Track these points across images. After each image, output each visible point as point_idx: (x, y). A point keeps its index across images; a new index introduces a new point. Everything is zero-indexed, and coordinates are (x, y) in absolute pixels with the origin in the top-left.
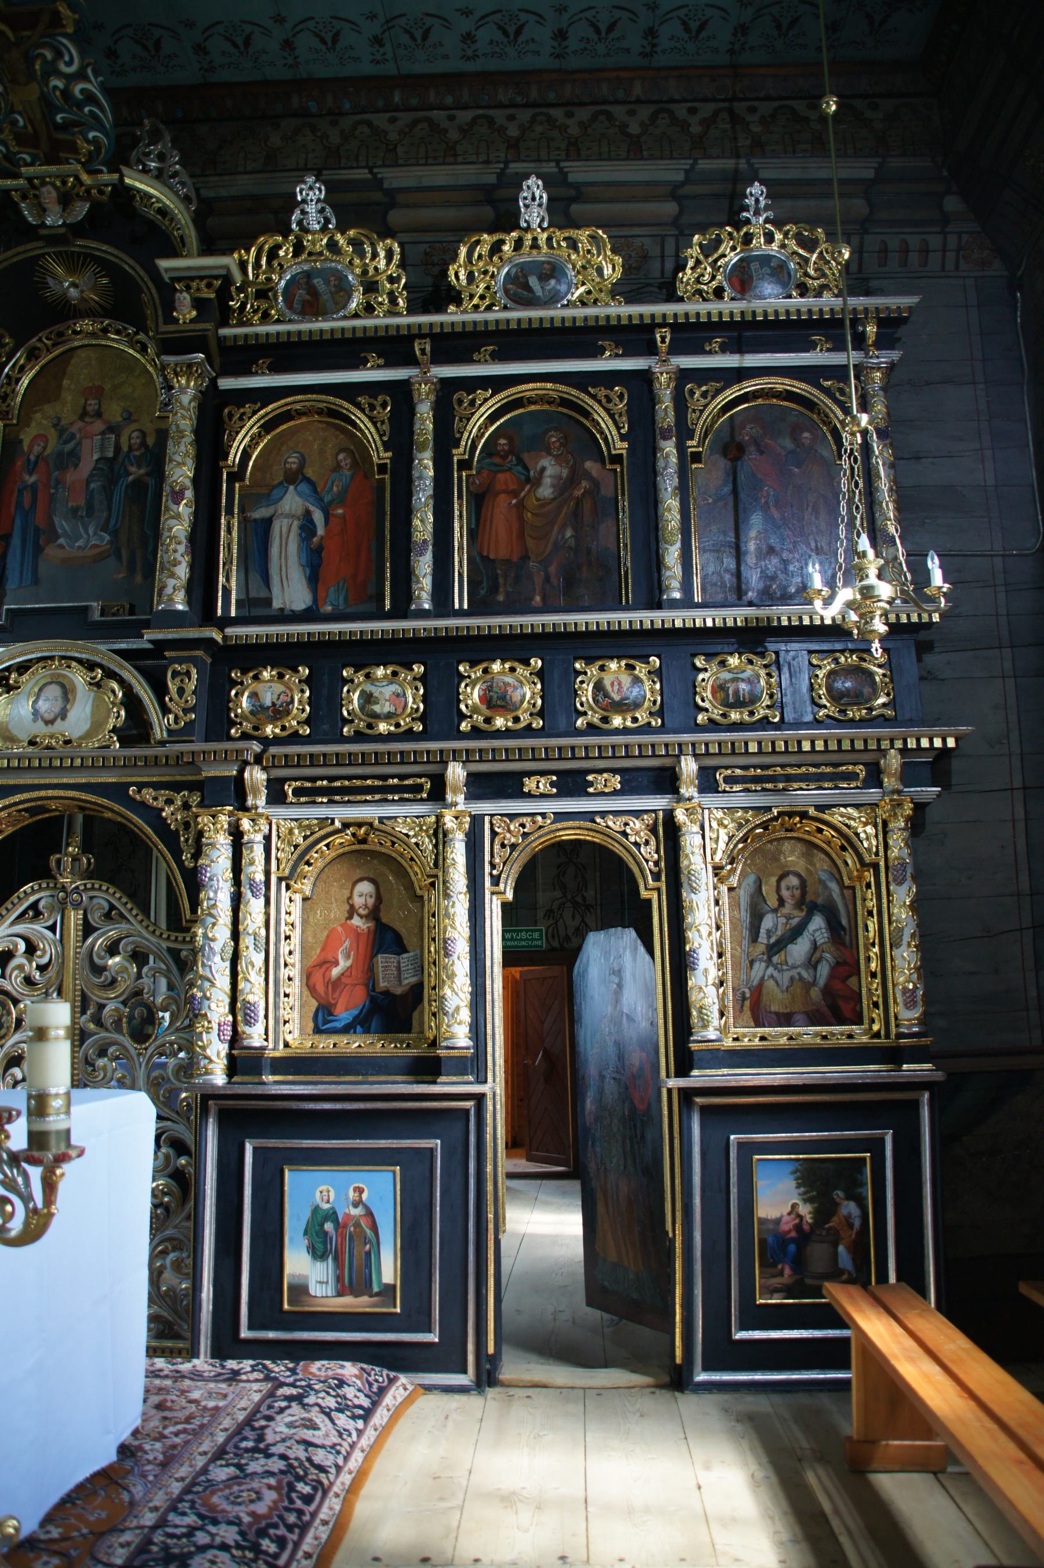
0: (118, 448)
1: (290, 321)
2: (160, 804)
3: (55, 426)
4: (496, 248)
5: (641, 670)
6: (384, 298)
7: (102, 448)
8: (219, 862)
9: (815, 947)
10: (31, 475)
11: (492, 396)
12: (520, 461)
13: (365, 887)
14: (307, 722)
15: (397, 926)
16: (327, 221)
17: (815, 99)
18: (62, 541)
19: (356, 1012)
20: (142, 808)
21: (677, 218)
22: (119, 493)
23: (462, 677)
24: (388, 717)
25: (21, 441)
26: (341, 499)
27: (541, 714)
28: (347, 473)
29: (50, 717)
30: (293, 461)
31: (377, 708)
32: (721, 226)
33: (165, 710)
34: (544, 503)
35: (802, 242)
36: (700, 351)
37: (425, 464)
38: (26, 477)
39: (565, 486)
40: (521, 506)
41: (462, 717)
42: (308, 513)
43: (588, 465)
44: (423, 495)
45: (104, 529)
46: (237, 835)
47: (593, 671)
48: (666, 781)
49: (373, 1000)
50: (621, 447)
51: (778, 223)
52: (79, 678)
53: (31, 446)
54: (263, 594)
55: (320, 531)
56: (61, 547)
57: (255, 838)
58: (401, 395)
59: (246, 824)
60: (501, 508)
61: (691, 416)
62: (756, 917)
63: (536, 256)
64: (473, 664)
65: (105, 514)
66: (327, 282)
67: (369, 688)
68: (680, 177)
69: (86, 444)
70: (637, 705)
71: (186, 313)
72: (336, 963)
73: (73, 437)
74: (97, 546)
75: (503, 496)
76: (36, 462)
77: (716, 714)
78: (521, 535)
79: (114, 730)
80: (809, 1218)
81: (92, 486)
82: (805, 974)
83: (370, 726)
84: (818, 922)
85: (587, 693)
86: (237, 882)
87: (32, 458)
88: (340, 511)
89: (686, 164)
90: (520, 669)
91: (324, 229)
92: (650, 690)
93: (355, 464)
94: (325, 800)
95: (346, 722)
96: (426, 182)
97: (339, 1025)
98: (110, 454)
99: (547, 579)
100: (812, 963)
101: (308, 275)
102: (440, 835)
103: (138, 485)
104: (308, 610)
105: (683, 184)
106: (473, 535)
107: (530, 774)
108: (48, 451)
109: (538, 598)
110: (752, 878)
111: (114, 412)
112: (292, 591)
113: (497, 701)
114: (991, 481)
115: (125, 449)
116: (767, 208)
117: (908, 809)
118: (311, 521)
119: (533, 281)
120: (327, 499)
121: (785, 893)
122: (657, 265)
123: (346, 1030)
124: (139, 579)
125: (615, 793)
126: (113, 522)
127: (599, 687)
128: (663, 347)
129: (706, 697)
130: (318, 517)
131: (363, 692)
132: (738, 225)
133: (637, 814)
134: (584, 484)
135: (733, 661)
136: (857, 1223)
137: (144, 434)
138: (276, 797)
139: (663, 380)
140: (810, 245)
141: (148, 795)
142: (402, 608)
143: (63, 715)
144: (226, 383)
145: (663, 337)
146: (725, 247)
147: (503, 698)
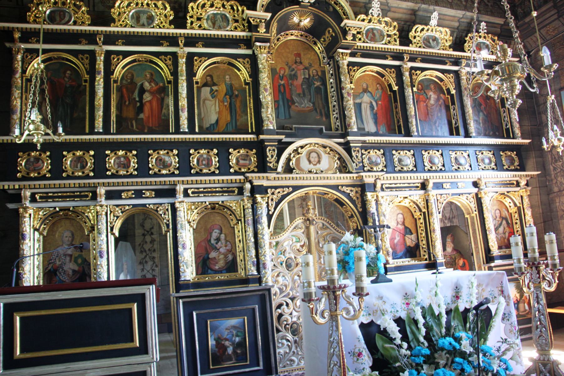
0: (309, 75)
1: (367, 42)
2: (348, 192)
3: (287, 65)
4: (423, 30)
7: (304, 74)
9: (504, 229)
10: (282, 81)
11: (422, 72)
12: (425, 92)
13: (400, 216)
15: (409, 227)
16: (379, 14)
17: (530, 13)
18: (296, 104)
19: (402, 253)
20: (343, 193)
21: (458, 27)
22: (312, 91)
25: (276, 69)
28: (380, 91)
29: (315, 163)
31: (403, 163)
33: (354, 162)
37: (409, 92)
38: (280, 81)
40: (427, 106)
41: (424, 166)
42: (371, 102)
43: (441, 95)
45: (310, 101)
46: (377, 201)
49: (406, 248)
50: (453, 92)
51: (487, 33)
52: (321, 150)
53: (280, 71)
54: (362, 127)
55: (376, 108)
56: (297, 106)
57: (381, 201)
58: (398, 70)
59: (380, 198)
65: (309, 97)
66: (378, 32)
67: (400, 157)
68: (461, 16)
69: (298, 72)
71: (349, 38)
72: (395, 239)
73: (293, 70)
74: (308, 107)
75: (422, 102)
76: (283, 77)
80: (519, 298)
81: (304, 87)
82: (504, 236)
83: (402, 168)
84: (504, 222)
87: (281, 75)
88: (380, 103)
89: (464, 12)
90: (438, 154)
91: (378, 16)
93: (382, 88)
94: (394, 190)
96: (400, 6)
97: (398, 257)
98: (307, 77)
100: (504, 233)
101: (372, 29)
103: (318, 89)
104: (375, 132)
105: (462, 18)
107: (445, 183)
108: (286, 74)
111: (306, 63)
112: (371, 127)
113: (431, 161)
115: (312, 75)
116: (485, 29)
118: (372, 105)
119: (431, 41)
120: (376, 98)
123: (401, 258)
124: (324, 119)
126: (312, 100)
127: (456, 159)
130: (374, 104)
131: (399, 158)
136: (528, 297)
137: (317, 72)
138: (382, 189)
141: (344, 189)
142: (408, 134)
143: (319, 162)
145: (464, 62)
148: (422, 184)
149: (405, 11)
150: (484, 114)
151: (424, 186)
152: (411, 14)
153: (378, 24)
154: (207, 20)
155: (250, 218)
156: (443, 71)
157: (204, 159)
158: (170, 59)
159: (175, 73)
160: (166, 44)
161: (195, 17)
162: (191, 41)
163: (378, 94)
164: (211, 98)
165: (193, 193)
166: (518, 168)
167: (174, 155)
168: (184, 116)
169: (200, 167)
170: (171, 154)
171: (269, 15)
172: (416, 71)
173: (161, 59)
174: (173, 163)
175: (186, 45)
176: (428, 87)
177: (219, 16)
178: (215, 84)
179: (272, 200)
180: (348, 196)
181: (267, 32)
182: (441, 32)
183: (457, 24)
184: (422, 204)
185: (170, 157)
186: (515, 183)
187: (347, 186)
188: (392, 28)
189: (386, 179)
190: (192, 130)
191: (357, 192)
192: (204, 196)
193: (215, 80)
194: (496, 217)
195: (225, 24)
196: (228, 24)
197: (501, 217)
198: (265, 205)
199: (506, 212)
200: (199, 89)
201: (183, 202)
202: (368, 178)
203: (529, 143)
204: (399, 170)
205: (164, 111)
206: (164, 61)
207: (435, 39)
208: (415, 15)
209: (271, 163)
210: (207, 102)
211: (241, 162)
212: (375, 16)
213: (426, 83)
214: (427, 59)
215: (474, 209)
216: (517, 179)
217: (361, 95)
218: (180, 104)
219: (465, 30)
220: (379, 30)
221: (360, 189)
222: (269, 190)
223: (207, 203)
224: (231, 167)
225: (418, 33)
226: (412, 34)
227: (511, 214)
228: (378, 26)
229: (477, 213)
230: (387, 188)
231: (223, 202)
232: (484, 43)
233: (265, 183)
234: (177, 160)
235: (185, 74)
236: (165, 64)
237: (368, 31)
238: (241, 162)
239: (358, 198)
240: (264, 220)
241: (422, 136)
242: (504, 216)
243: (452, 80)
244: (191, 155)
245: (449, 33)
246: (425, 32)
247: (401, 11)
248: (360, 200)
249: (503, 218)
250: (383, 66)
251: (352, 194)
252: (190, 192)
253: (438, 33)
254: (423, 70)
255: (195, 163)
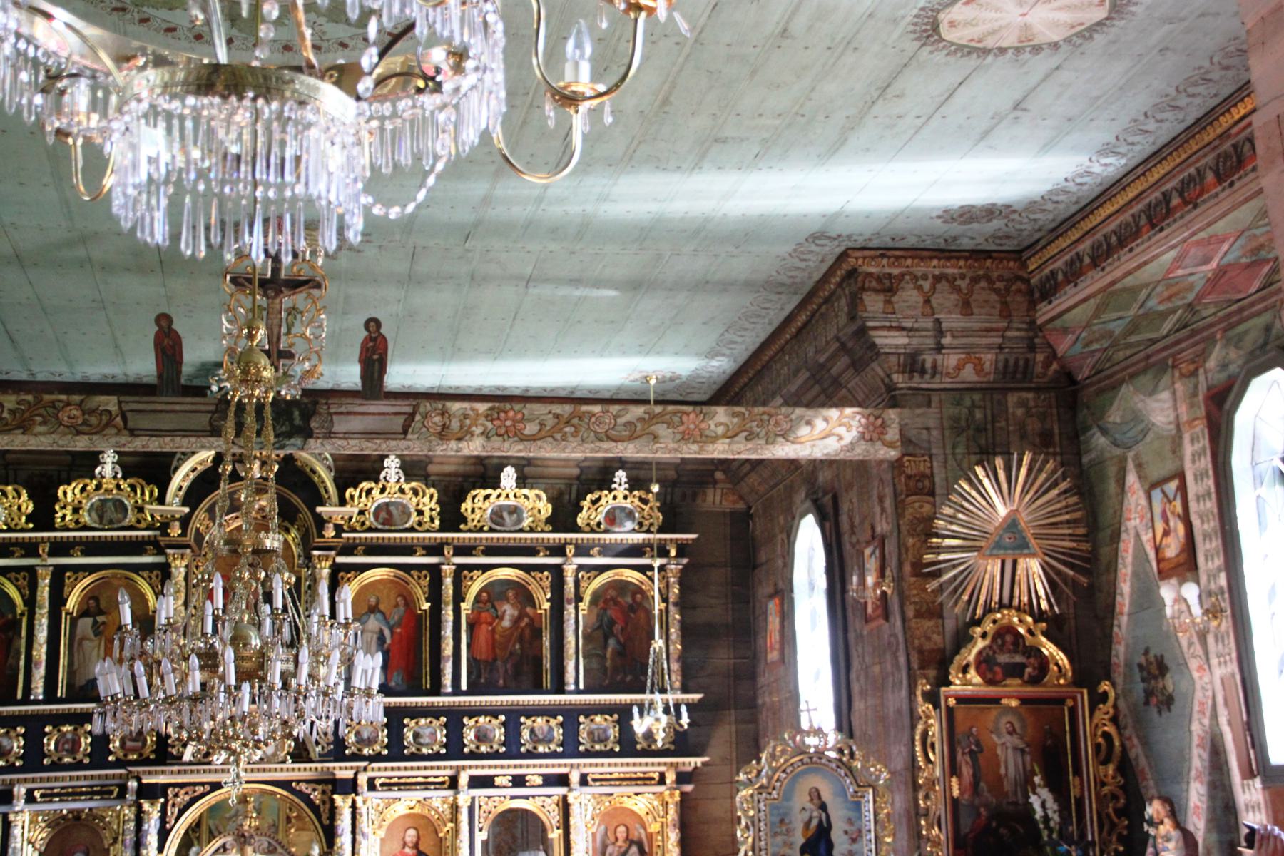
2: (309, 791)
4: (487, 497)
5: (553, 722)
6: (427, 519)
8: (344, 823)
12: (494, 607)
13: (412, 832)
14: (387, 747)
20: (300, 794)
23: (464, 725)
24: (427, 745)
26: (399, 624)
27: (504, 744)
28: (402, 608)
30: (373, 601)
31: (422, 741)
32: (601, 490)
34: (505, 630)
35: (641, 500)
36: (590, 556)
39: (516, 621)
40: (493, 631)
41: (465, 745)
42: (381, 631)
43: (529, 610)
44: (448, 632)
46: (354, 806)
47: (529, 722)
48: (563, 780)
50: (547, 606)
55: (389, 641)
58: (435, 571)
60: (484, 630)
61: (582, 589)
62: (605, 847)
63: (507, 503)
64: (470, 718)
67: (417, 729)
70: (550, 741)
71: (330, 532)
77: (588, 746)
78: (493, 648)
79: (288, 753)
83: (418, 750)
84: (634, 849)
85: (526, 734)
86: (354, 832)
91: (398, 481)
92: (558, 734)
93: (407, 604)
95: (406, 747)
99: (506, 671)
101: (387, 504)
102: (455, 808)
106: (469, 646)
109: (501, 682)
110: (602, 828)
114: (730, 620)
117: (677, 798)
119: (505, 515)
121: (619, 835)
122: (567, 497)
125: (539, 786)
127: (532, 731)
128: (569, 554)
129: (583, 736)
130: (387, 633)
132: (611, 491)
133: (549, 796)
134: (526, 620)
135: (598, 719)
138: (371, 785)
139: (569, 571)
140: (645, 501)
141: (303, 787)
142: (436, 690)
144: (340, 560)
145: (570, 550)
146: (603, 501)
147: (485, 736)
148: (451, 777)
149: (461, 461)
150: (618, 642)
151: (453, 783)
152: (474, 464)
153: (398, 495)
154: (89, 511)
155: (130, 838)
156: (527, 568)
157: (67, 741)
158: (24, 578)
159: (31, 603)
160: (19, 551)
161: (70, 508)
162: (60, 548)
163: (397, 615)
164: (92, 636)
165: (42, 796)
166: (672, 747)
167: (18, 735)
168: (39, 673)
169: (60, 755)
170: (13, 734)
171: (187, 510)
172: (471, 571)
173: (9, 579)
174: (16, 749)
175: (52, 554)
176: (503, 597)
177: (110, 504)
178: (101, 612)
179: (173, 805)
180: (306, 798)
181: (184, 534)
182: (526, 497)
183: (576, 471)
184: (448, 815)
185: (10, 738)
186: (656, 776)
187: (307, 781)
188: (426, 499)
189: (382, 771)
190: (50, 697)
191: (324, 792)
192: (61, 801)
193: (103, 605)
194: (617, 839)
195: (120, 516)
196: (125, 517)
197: (627, 838)
198: (155, 815)
199: (642, 831)
200: (74, 622)
201: (22, 811)
202: (343, 771)
203: (700, 700)
204: (413, 754)
205: (11, 661)
206: (14, 582)
207: (515, 510)
208: (484, 465)
209: (173, 747)
210: (87, 644)
211: (129, 744)
212: (393, 479)
213: (498, 589)
214: (491, 551)
215: (554, 822)
216: (663, 769)
217: (365, 618)
218: (34, 653)
219: (594, 480)
220: (401, 504)
221: (330, 787)
222: (170, 791)
223: (65, 812)
224: (111, 753)
225: (478, 505)
226: (466, 506)
227: (651, 834)
228: (397, 498)
229: (561, 831)
230: (383, 785)
231: (91, 809)
232: (623, 509)
233: (162, 779)
234: (22, 743)
235: (47, 604)
236: (16, 586)
237: (379, 508)
238: (129, 744)
239: (324, 802)
240: (152, 839)
241: (469, 693)
242: (635, 839)
243: (547, 583)
244: (46, 734)
245: (544, 496)
246: (493, 498)
247: (456, 460)
248: (328, 806)
249: (632, 842)
250: (406, 568)
251: (316, 796)
252: (37, 794)
253: (522, 500)
254: (485, 568)
255: (52, 747)
